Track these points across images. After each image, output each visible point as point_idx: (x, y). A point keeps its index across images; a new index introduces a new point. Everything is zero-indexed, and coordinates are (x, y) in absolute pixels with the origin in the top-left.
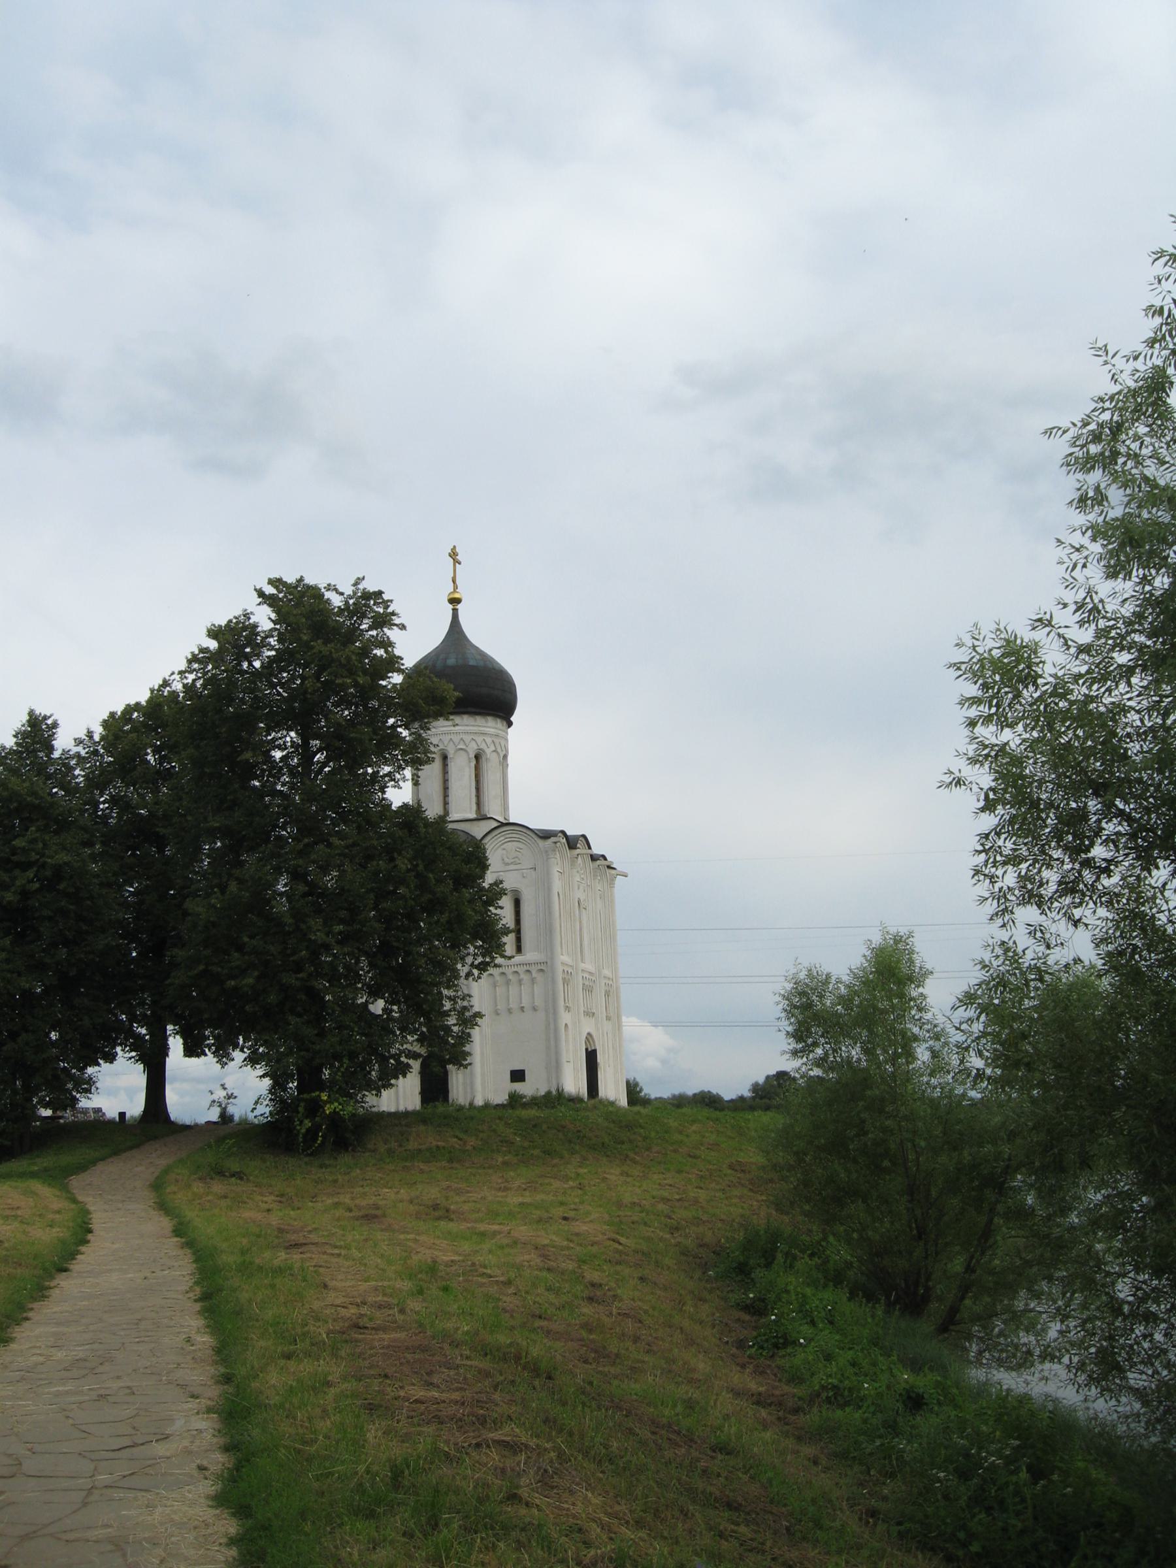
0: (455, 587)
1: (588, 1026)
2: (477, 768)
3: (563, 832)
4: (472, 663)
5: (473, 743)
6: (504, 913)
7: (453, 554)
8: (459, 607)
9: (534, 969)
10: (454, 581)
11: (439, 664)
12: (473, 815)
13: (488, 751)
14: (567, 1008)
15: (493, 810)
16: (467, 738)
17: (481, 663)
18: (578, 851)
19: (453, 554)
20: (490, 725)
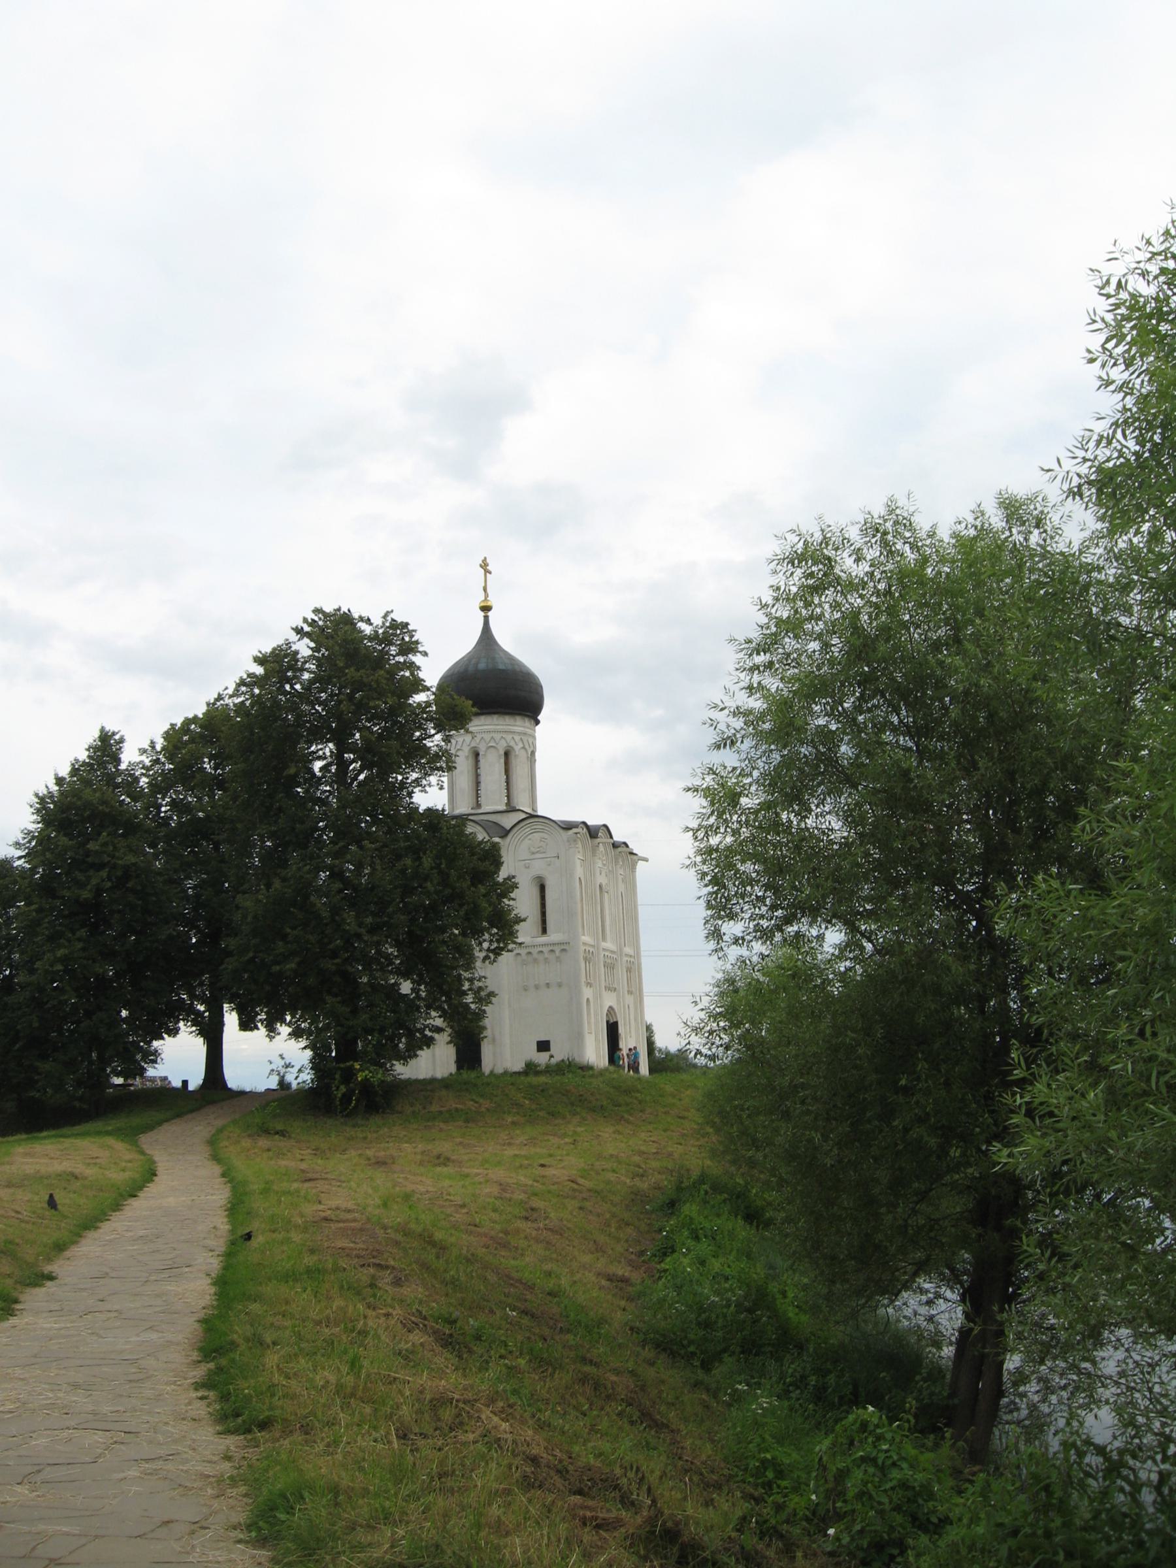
0: (486, 595)
1: (609, 1000)
2: (507, 763)
3: (584, 823)
4: (501, 667)
5: (503, 742)
6: (523, 903)
7: (484, 565)
8: (490, 614)
9: (557, 949)
10: (485, 589)
11: (471, 668)
12: (503, 808)
13: (517, 748)
14: (589, 984)
15: (523, 805)
16: (497, 736)
17: (510, 667)
18: (598, 840)
19: (484, 565)
20: (518, 724)
